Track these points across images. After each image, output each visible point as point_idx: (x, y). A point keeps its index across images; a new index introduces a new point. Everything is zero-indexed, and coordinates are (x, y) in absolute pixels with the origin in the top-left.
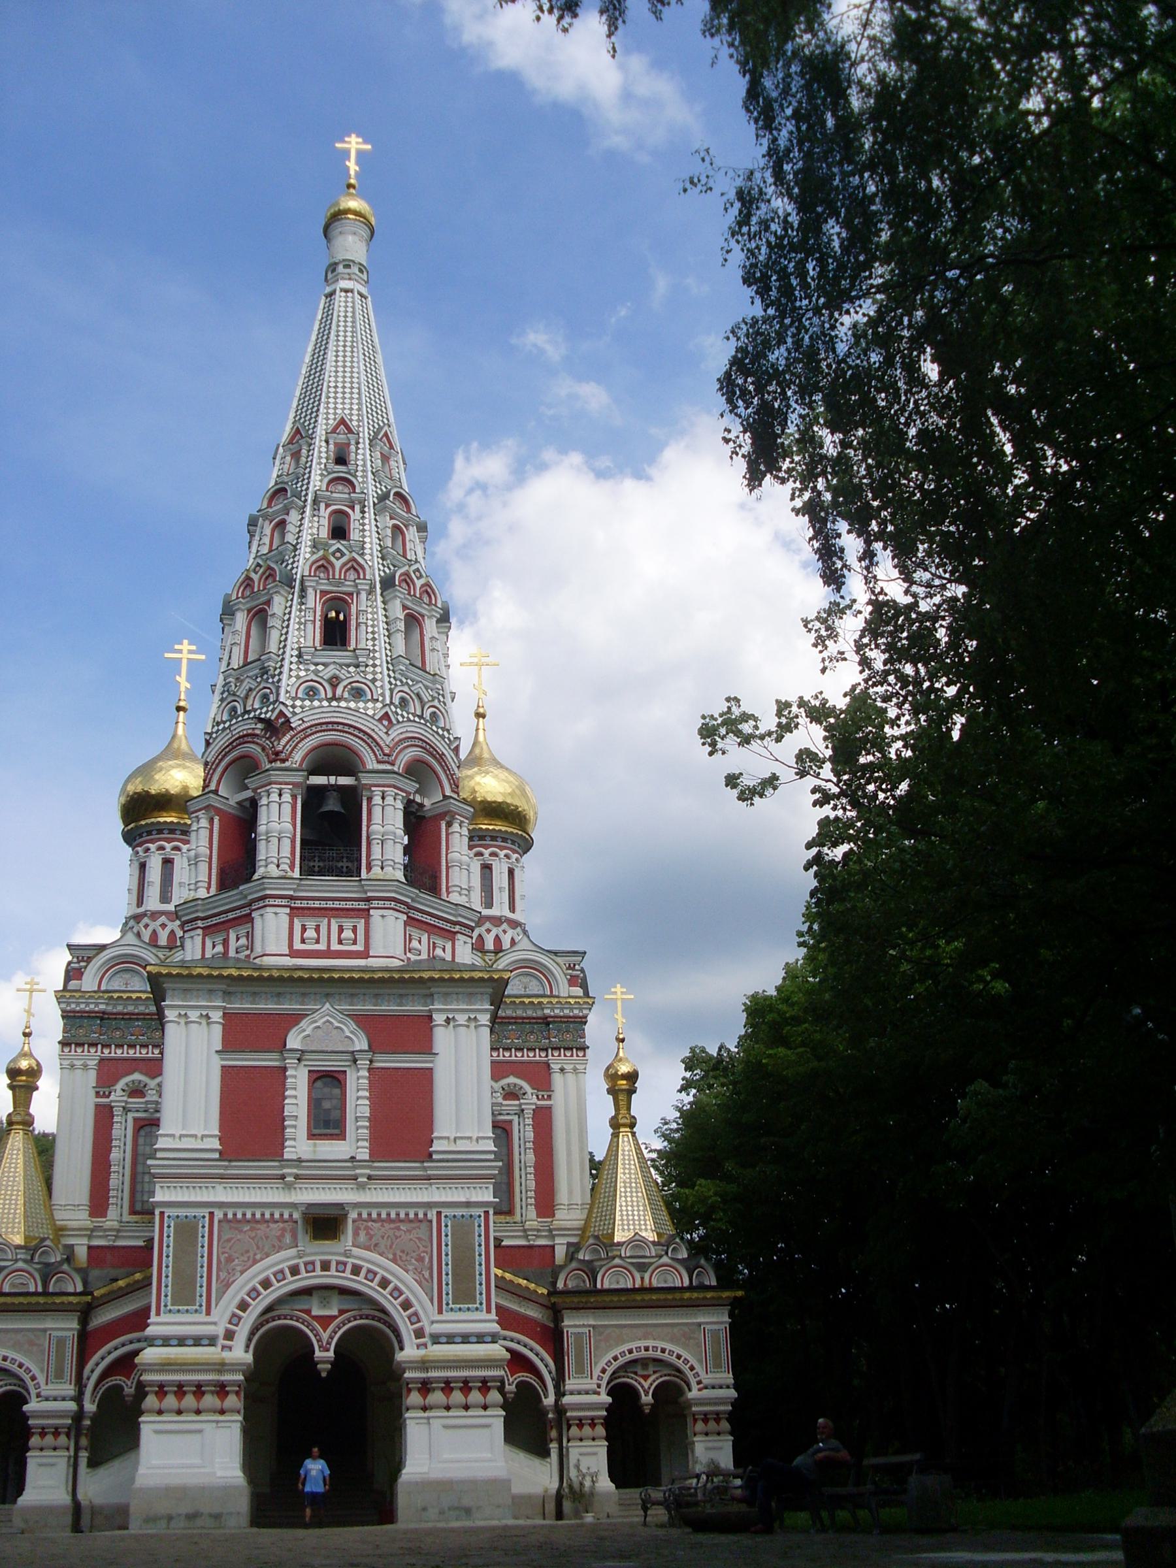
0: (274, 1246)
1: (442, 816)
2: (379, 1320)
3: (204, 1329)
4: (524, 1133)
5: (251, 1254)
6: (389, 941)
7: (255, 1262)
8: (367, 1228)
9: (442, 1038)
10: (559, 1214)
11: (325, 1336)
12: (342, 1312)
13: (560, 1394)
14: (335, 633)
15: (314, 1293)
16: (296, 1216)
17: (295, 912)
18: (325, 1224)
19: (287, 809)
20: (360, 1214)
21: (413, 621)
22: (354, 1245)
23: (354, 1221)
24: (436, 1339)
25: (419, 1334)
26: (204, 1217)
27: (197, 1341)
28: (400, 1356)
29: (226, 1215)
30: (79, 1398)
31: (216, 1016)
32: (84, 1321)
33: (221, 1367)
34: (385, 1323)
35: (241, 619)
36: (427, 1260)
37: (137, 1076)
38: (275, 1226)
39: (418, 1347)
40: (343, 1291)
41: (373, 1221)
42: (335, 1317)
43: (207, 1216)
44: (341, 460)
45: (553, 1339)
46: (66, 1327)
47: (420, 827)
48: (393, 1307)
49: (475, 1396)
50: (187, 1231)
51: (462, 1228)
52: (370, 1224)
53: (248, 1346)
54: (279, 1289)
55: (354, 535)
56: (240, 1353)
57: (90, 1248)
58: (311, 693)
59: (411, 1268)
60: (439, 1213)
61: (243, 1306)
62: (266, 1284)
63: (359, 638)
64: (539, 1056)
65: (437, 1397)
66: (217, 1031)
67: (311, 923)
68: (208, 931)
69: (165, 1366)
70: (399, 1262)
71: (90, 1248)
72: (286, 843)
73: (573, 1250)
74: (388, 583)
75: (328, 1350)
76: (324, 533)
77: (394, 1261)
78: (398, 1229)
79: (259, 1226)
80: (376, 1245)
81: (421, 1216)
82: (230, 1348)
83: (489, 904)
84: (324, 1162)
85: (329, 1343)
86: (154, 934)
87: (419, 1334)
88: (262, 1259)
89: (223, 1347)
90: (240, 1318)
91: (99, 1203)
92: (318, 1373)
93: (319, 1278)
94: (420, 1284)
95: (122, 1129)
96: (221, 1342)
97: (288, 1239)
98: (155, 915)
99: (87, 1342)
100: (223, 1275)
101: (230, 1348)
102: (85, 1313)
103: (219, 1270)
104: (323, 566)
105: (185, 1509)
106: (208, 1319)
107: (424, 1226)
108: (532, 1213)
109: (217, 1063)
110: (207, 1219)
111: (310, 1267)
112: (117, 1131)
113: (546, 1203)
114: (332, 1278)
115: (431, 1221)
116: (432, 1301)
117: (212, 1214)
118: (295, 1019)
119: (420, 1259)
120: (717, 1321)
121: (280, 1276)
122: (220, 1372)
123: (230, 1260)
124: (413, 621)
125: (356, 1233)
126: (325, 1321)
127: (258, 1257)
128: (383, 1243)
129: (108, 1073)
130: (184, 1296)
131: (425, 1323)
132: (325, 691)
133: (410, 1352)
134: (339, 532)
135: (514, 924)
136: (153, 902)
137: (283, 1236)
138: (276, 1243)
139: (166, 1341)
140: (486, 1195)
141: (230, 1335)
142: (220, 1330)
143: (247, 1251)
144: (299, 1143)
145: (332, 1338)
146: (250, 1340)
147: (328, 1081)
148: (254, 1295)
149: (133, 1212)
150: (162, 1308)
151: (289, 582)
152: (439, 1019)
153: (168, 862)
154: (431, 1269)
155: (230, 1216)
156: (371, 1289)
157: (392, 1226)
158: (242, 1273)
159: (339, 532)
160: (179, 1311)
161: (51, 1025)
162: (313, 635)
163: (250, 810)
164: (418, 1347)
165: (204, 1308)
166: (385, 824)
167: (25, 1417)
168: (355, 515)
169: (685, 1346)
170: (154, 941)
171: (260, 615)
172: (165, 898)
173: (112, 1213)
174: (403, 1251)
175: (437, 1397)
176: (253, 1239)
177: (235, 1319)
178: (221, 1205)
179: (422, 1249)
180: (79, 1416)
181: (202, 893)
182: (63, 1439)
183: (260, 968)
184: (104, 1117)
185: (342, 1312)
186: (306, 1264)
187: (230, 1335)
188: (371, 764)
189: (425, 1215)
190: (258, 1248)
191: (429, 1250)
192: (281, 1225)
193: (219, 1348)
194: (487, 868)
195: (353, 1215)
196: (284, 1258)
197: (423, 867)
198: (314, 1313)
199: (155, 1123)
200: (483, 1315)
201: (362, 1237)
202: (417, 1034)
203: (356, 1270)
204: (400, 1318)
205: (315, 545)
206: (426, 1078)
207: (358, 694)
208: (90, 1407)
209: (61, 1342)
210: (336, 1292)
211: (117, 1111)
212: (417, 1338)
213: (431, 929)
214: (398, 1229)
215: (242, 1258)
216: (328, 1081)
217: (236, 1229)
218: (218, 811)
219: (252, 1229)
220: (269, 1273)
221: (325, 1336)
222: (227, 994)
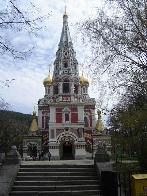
1: (78, 86)
3: (55, 141)
4: (89, 118)
6: (73, 100)
9: (78, 110)
10: (93, 127)
13: (93, 146)
14: (66, 66)
16: (64, 129)
17: (63, 97)
18: (67, 129)
19: (61, 86)
21: (75, 64)
24: (78, 141)
25: (77, 141)
27: (54, 142)
28: (75, 143)
30: (42, 147)
31: (55, 108)
32: (42, 139)
33: (56, 144)
35: (56, 65)
37: (47, 113)
40: (69, 136)
44: (66, 46)
45: (92, 141)
46: (40, 140)
47: (76, 87)
48: (74, 138)
49: (82, 147)
50: (53, 130)
51: (81, 130)
54: (62, 136)
55: (68, 55)
56: (58, 143)
57: (42, 132)
58: (64, 73)
61: (59, 138)
63: (69, 66)
64: (89, 110)
65: (79, 147)
66: (55, 110)
67: (64, 98)
68: (54, 99)
69: (51, 144)
71: (42, 132)
72: (62, 90)
73: (94, 131)
74: (71, 60)
76: (64, 55)
83: (84, 93)
84: (68, 123)
86: (48, 97)
87: (77, 141)
91: (43, 127)
93: (66, 135)
95: (45, 119)
98: (48, 95)
99: (43, 142)
102: (42, 138)
104: (64, 59)
105: (54, 158)
108: (89, 127)
109: (55, 113)
112: (45, 119)
113: (91, 126)
114: (68, 135)
118: (63, 108)
120: (109, 138)
124: (75, 64)
126: (67, 140)
129: (44, 113)
130: (53, 137)
132: (65, 73)
133: (76, 143)
134: (66, 54)
135: (87, 95)
136: (47, 94)
139: (51, 142)
140: (84, 126)
141: (57, 141)
144: (64, 121)
147: (67, 116)
149: (47, 127)
151: (61, 60)
152: (78, 108)
153: (49, 89)
156: (72, 136)
159: (66, 54)
161: (37, 107)
162: (64, 66)
163: (58, 86)
166: (72, 87)
167: (36, 149)
168: (68, 52)
169: (106, 141)
170: (48, 97)
171: (58, 64)
172: (49, 93)
173: (45, 128)
175: (79, 147)
177: (58, 140)
178: (56, 128)
180: (42, 149)
181: (53, 95)
182: (40, 151)
183: (59, 103)
184: (43, 117)
187: (57, 141)
188: (70, 80)
194: (84, 89)
195: (70, 129)
196: (63, 133)
197: (76, 91)
199: (49, 118)
200: (83, 139)
202: (76, 110)
203: (70, 134)
204: (75, 139)
205: (63, 56)
206: (77, 114)
207: (69, 73)
208: (43, 148)
209: (40, 141)
211: (45, 117)
213: (77, 98)
216: (67, 116)
218: (54, 86)
220: (61, 135)
222: (56, 106)
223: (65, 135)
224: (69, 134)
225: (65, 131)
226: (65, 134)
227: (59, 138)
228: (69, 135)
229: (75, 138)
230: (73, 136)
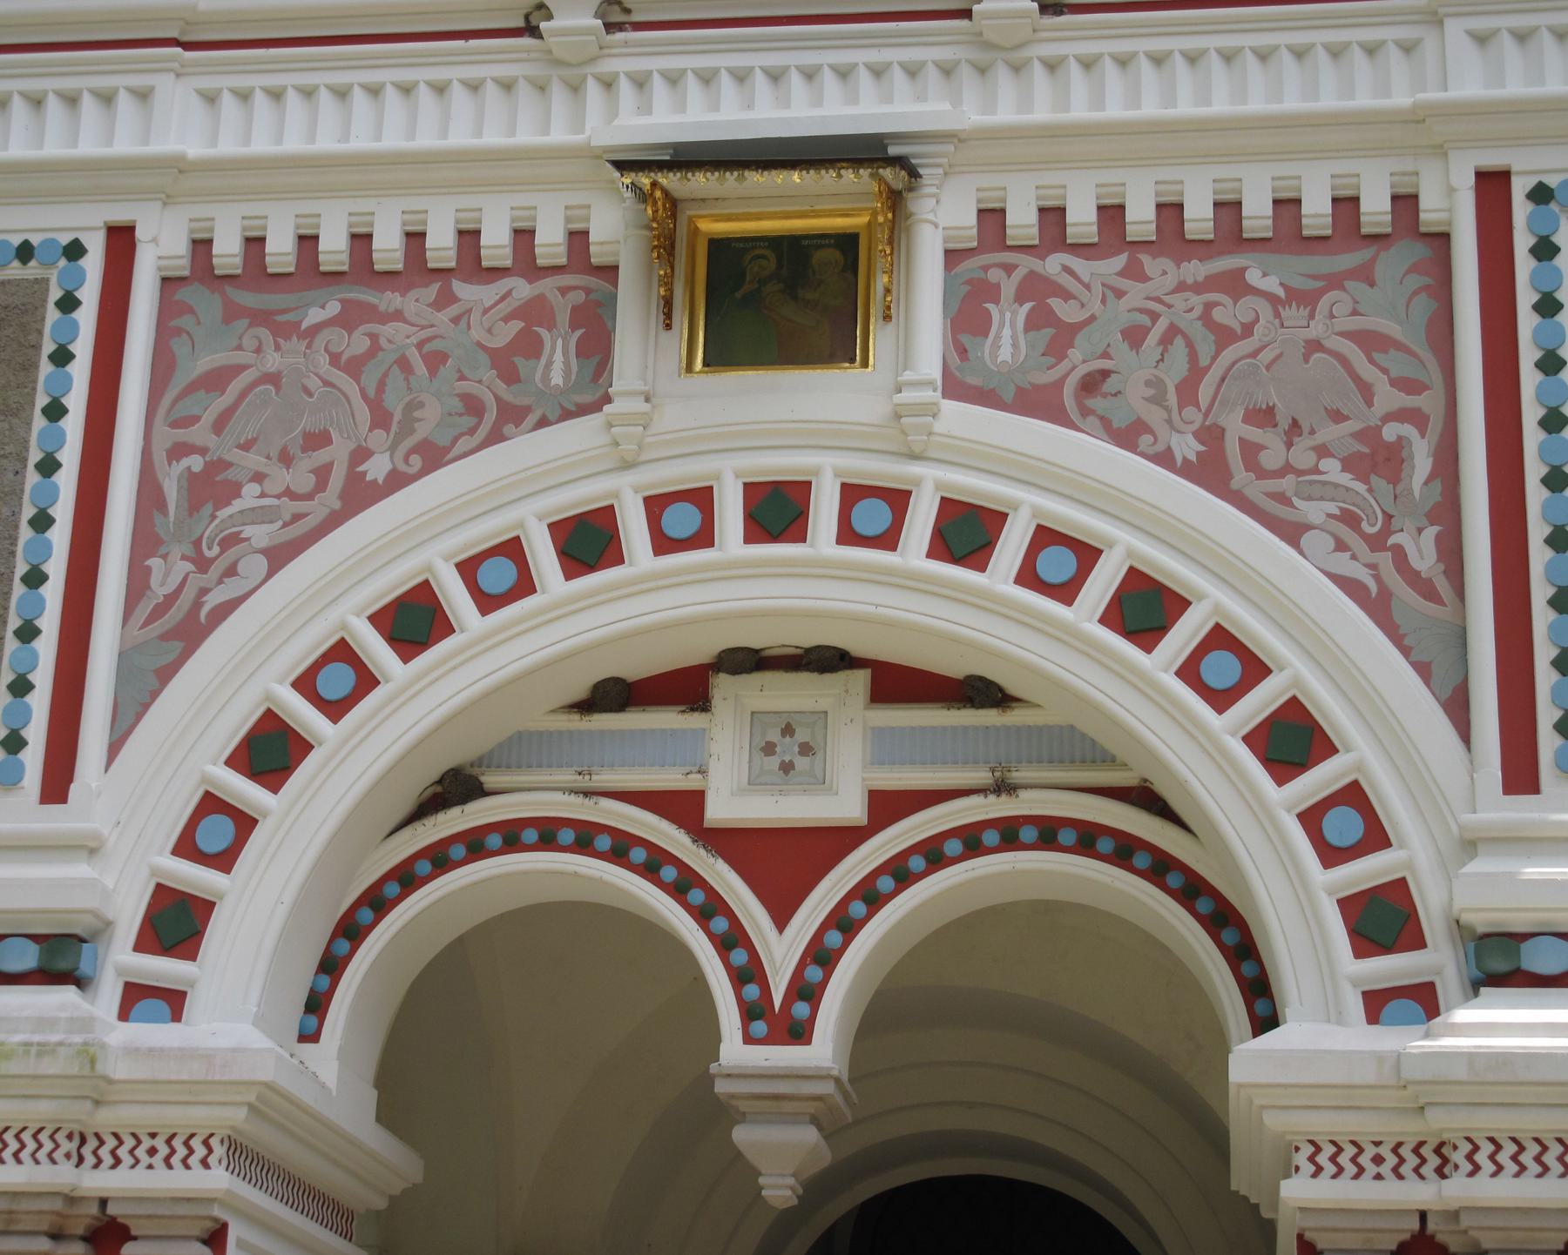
0: (473, 406)
2: (1125, 851)
5: (338, 453)
8: (1036, 289)
11: (781, 951)
12: (888, 807)
15: (723, 686)
16: (613, 225)
20: (992, 217)
22: (954, 387)
23: (953, 256)
24: (1501, 962)
25: (1382, 920)
26: (75, 251)
29: (202, 246)
34: (1160, 868)
36: (1422, 462)
38: (485, 294)
39: (1376, 1004)
41: (1080, 249)
42: (843, 839)
43: (96, 247)
48: (1206, 758)
52: (1053, 265)
53: (317, 1005)
59: (1314, 511)
60: (1493, 184)
61: (270, 751)
62: (414, 621)
70: (1241, 477)
75: (800, 1033)
77: (1209, 471)
78: (1235, 284)
79: (389, 300)
80: (1092, 384)
81: (1376, 208)
82: (174, 1001)
85: (806, 991)
87: (1382, 920)
88: (397, 481)
89: (134, 996)
90: (245, 823)
92: (740, 1169)
93: (739, 589)
94: (1378, 607)
96: (122, 958)
97: (557, 363)
100: (167, 573)
101: (174, 1001)
103: (144, 542)
106: (56, 820)
107: (1395, 263)
110: (93, 263)
111: (682, 520)
115: (1443, 239)
116: (1458, 708)
117: (121, 240)
119: (1379, 460)
121: (497, 576)
122: (84, 1144)
123: (212, 487)
125: (968, 317)
126: (784, 861)
127: (377, 468)
128: (1137, 378)
131: (1414, 854)
137: (529, 345)
138: (486, 384)
141: (176, 923)
142: (114, 890)
145: (821, 956)
146: (331, 966)
148: (336, 682)
154: (1449, 514)
155: (228, 250)
156: (1062, 652)
157: (1196, 270)
158: (279, 557)
164: (1376, 1004)
174: (1263, 416)
176: (354, 367)
178: (171, 177)
179: (1388, 398)
185: (888, 807)
186: (656, 505)
189: (1405, 203)
190: (381, 419)
191: (1431, 402)
192: (522, 289)
193: (109, 993)
198: (719, 811)
201: (1008, 341)
203: (966, 533)
210: (860, 680)
212: (1366, 942)
214: (1235, 284)
215: (281, 478)
217: (261, 318)
219: (349, 318)
221: (781, 951)
223: (652, 605)
224: (874, 513)
225: (646, 352)
226: (681, 520)
227: (270, 751)
228: (909, 601)
229: (1291, 741)
230: (1144, 609)
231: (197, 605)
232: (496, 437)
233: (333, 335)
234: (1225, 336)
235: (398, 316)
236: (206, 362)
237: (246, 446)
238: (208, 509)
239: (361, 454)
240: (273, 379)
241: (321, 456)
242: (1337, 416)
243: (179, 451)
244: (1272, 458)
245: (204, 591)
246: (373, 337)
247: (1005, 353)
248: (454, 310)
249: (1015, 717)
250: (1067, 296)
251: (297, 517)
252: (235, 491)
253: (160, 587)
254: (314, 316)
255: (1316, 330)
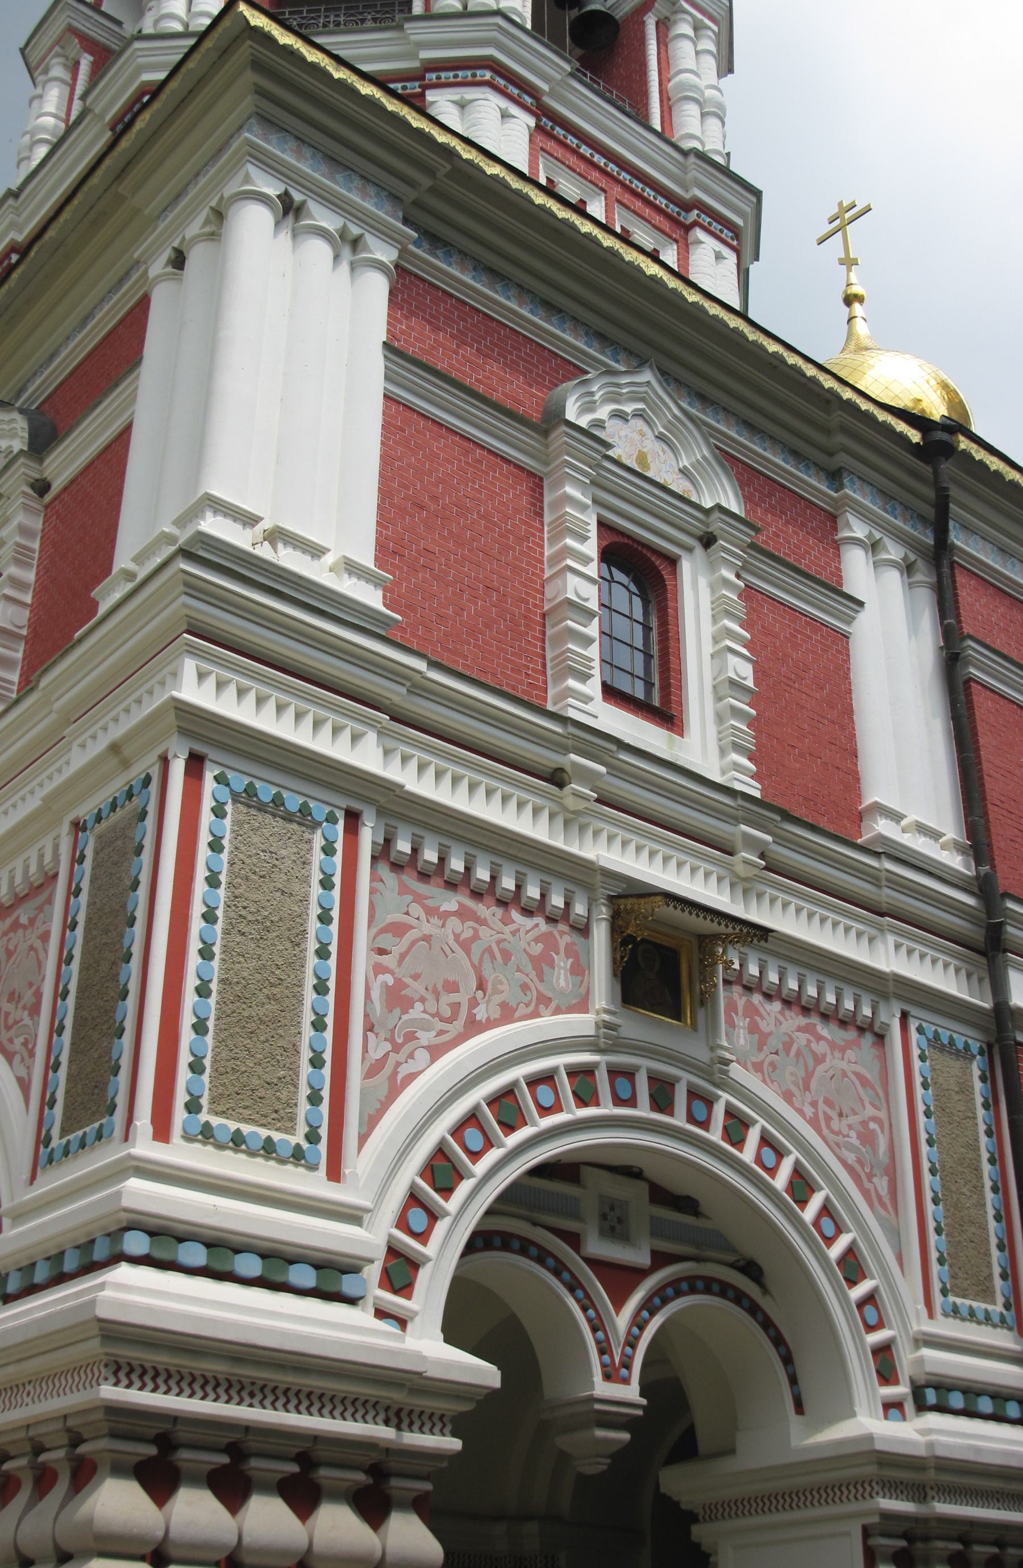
7: (474, 1027)
70: (825, 1131)
88: (490, 1024)
143: (452, 987)
150: (180, 1115)
158: (436, 1052)
160: (237, 1141)
165: (323, 1147)
176: (466, 946)
187: (401, 1270)
191: (882, 1114)
217: (419, 899)
219: (463, 914)
231: (395, 1073)
232: (535, 1014)
233: (454, 923)
234: (819, 1060)
235: (483, 922)
236: (391, 918)
237: (416, 977)
238: (397, 1011)
239: (473, 1003)
240: (427, 938)
241: (454, 997)
242: (855, 1113)
243: (379, 969)
244: (835, 1125)
245: (398, 1064)
246: (476, 930)
247: (742, 1042)
248: (512, 927)
249: (700, 1223)
250: (763, 1018)
251: (441, 1033)
252: (407, 1004)
253: (376, 1054)
254: (445, 907)
255: (844, 1065)
